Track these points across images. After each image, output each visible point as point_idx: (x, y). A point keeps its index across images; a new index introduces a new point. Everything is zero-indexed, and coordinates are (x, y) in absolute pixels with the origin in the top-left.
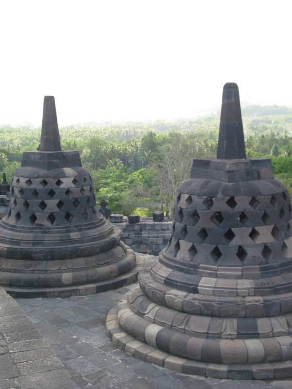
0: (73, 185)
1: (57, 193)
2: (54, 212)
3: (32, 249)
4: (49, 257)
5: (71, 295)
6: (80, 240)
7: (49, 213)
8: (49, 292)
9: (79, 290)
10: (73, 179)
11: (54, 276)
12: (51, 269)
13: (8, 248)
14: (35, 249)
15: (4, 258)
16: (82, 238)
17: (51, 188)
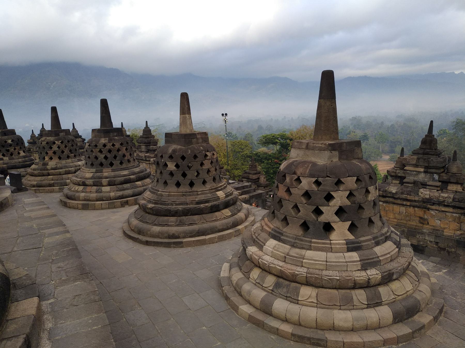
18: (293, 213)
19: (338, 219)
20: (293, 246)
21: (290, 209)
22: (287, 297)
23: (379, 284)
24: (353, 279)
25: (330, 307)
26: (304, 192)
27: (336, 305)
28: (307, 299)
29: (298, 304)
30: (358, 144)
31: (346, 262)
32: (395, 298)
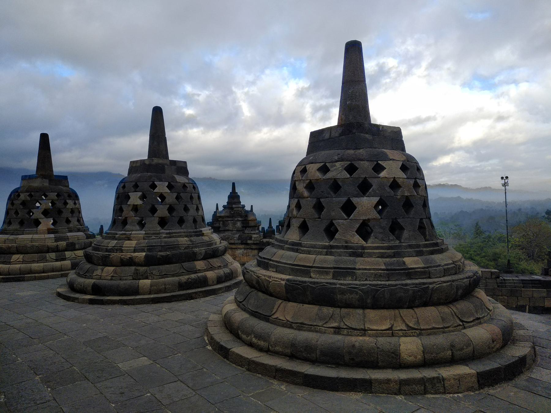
0: (402, 175)
2: (369, 220)
5: (426, 392)
6: (424, 273)
7: (361, 221)
8: (376, 380)
9: (444, 379)
10: (400, 164)
11: (384, 342)
12: (375, 327)
13: (288, 280)
14: (341, 284)
15: (279, 298)
16: (428, 268)
19: (44, 217)
20: (12, 235)
22: (3, 262)
25: (31, 262)
26: (21, 201)
28: (17, 260)
29: (10, 264)
30: (65, 178)
31: (45, 238)
32: (76, 257)
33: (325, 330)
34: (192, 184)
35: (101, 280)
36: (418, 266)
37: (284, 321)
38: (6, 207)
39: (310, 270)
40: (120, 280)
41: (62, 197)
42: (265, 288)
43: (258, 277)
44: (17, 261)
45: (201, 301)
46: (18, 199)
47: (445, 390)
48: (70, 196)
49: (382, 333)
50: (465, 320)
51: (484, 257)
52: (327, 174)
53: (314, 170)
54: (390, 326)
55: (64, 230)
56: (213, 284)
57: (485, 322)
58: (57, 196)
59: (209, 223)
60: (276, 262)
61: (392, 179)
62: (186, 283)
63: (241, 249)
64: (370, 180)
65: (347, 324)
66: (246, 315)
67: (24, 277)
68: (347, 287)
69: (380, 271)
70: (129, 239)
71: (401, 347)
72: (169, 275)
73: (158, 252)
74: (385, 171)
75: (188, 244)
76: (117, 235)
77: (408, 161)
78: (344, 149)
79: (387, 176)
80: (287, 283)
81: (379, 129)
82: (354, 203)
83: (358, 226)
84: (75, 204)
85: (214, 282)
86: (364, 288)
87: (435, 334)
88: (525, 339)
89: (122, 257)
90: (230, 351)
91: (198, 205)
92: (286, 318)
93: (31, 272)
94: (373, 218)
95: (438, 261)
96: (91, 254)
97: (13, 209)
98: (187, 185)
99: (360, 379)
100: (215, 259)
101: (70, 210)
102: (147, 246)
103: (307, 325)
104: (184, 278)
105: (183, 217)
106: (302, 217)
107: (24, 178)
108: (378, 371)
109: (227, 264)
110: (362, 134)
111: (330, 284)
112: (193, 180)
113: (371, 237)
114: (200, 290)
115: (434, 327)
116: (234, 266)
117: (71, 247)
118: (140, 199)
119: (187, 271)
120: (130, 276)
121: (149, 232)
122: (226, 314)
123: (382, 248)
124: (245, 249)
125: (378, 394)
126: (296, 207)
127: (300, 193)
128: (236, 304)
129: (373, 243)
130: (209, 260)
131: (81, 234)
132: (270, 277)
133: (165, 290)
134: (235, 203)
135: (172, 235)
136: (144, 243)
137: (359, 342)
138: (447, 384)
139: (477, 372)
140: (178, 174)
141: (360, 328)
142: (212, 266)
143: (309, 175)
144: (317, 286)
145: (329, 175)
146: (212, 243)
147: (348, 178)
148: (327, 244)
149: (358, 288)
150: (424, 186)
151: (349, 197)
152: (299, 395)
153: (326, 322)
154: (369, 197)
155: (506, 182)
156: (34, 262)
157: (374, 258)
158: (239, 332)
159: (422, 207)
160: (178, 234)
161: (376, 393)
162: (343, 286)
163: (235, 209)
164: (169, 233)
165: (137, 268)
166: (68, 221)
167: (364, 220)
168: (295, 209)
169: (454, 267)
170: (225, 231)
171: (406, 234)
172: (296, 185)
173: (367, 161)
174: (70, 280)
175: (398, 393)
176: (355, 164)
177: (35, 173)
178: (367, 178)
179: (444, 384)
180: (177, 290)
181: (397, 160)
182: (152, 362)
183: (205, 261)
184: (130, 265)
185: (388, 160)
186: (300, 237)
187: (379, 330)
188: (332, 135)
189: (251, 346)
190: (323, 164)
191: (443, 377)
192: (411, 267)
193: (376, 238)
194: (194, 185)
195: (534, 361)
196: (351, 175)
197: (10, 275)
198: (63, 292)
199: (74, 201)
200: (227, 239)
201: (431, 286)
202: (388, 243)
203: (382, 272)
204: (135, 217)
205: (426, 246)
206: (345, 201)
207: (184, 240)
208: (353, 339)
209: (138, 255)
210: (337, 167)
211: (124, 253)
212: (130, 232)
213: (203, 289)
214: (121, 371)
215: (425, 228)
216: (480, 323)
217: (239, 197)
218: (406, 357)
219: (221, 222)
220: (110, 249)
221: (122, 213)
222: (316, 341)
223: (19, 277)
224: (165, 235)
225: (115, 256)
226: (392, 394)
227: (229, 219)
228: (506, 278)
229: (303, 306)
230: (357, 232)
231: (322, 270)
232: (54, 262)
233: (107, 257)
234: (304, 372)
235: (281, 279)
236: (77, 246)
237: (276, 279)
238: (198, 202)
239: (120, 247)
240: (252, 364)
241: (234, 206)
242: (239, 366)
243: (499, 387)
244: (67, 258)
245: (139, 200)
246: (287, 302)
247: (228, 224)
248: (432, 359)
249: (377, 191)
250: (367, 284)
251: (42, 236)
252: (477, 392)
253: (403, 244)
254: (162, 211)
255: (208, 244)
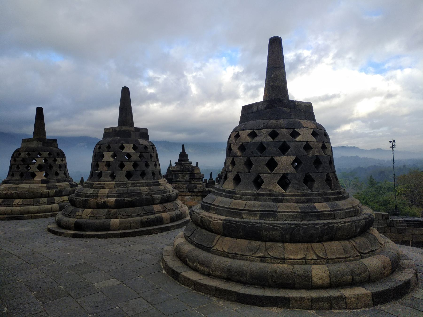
0: (313, 139)
1: (292, 148)
2: (287, 174)
3: (261, 223)
4: (288, 236)
5: (331, 308)
7: (282, 175)
8: (293, 298)
9: (346, 298)
10: (312, 131)
11: (299, 268)
12: (292, 257)
13: (225, 220)
14: (266, 223)
15: (218, 234)
16: (333, 211)
17: (283, 140)
18: (16, 170)
20: (14, 184)
21: (15, 168)
22: (7, 205)
23: (55, 196)
24: (40, 192)
26: (21, 159)
27: (32, 204)
28: (17, 203)
29: (12, 207)
30: (55, 141)
31: (39, 187)
33: (253, 259)
34: (151, 145)
35: (81, 219)
36: (325, 210)
37: (222, 251)
38: (10, 162)
39: (242, 212)
40: (96, 219)
41: (52, 156)
42: (207, 225)
43: (202, 217)
44: (18, 204)
45: (158, 236)
46: (19, 157)
47: (347, 306)
48: (58, 155)
49: (297, 262)
50: (362, 252)
51: (377, 202)
52: (255, 138)
53: (245, 135)
54: (304, 256)
55: (54, 181)
56: (167, 223)
57: (378, 254)
58: (48, 154)
59: (165, 176)
60: (216, 206)
61: (305, 143)
62: (146, 222)
63: (189, 195)
64: (288, 143)
65: (271, 255)
66: (192, 247)
67: (23, 217)
68: (271, 226)
69: (296, 214)
70: (103, 188)
71: (312, 273)
72: (133, 216)
73: (126, 198)
74: (300, 136)
75: (148, 192)
76: (94, 184)
77: (317, 129)
78: (268, 119)
79: (301, 140)
80: (224, 222)
81: (295, 104)
82: (276, 161)
83: (279, 179)
84: (62, 160)
85: (167, 221)
86: (283, 226)
87: (338, 262)
88: (409, 267)
89: (98, 201)
90: (180, 275)
91: (156, 162)
92: (223, 249)
93: (28, 212)
94: (290, 172)
95: (341, 206)
96: (74, 199)
97: (15, 164)
98: (148, 147)
99: (280, 297)
100: (169, 203)
101: (58, 165)
102: (117, 193)
103: (239, 255)
104: (145, 218)
105: (145, 171)
106: (236, 172)
107: (24, 141)
108: (295, 291)
109: (178, 207)
110: (282, 108)
111: (258, 223)
112: (152, 143)
113: (289, 187)
114: (157, 227)
115: (338, 257)
116: (183, 209)
117: (59, 193)
118: (112, 157)
119: (147, 212)
120: (104, 216)
121: (119, 182)
122: (177, 246)
123: (298, 195)
124: (191, 195)
125: (294, 309)
126: (231, 163)
127: (235, 153)
128: (184, 238)
129: (290, 191)
130: (164, 204)
131: (67, 183)
132: (211, 217)
133: (130, 226)
134: (184, 161)
135: (136, 185)
136: (115, 191)
137: (280, 269)
138: (348, 301)
139: (372, 293)
140: (140, 138)
141: (281, 257)
142: (166, 208)
143: (241, 139)
144: (248, 225)
145: (257, 139)
146: (167, 191)
147: (272, 142)
148: (255, 192)
149: (279, 226)
150: (330, 148)
151: (272, 156)
152: (233, 309)
153: (255, 253)
154: (287, 156)
155: (393, 145)
156: (30, 205)
157: (292, 203)
158: (187, 260)
159: (328, 164)
160: (141, 184)
161: (293, 308)
162: (267, 225)
163: (184, 165)
164: (134, 183)
165: (109, 210)
166: (57, 174)
167: (284, 174)
168: (230, 164)
169: (354, 211)
170: (176, 181)
171: (316, 185)
172: (231, 146)
173: (286, 128)
174: (58, 219)
175: (311, 308)
176: (276, 131)
177: (32, 137)
178: (286, 142)
179: (346, 302)
180: (140, 227)
181: (309, 128)
182: (120, 283)
183: (161, 205)
184: (104, 208)
185: (302, 128)
186: (234, 187)
187: (296, 259)
188: (259, 109)
189: (197, 271)
190: (252, 130)
191: (345, 296)
192: (320, 210)
193: (293, 188)
194: (153, 146)
195: (417, 284)
196: (273, 139)
197: (12, 214)
198: (52, 228)
199: (61, 158)
200: (178, 188)
201: (336, 225)
202: (302, 192)
203: (298, 214)
204: (108, 171)
205: (332, 194)
206: (269, 159)
207: (145, 189)
208: (275, 266)
209: (110, 200)
210: (263, 133)
211: (99, 198)
212: (104, 183)
213: (160, 227)
214: (96, 289)
215: (331, 180)
216: (374, 254)
217: (187, 156)
218: (316, 280)
219: (174, 175)
220: (89, 195)
221: (98, 168)
222: (246, 267)
223: (19, 217)
224: (131, 185)
225: (92, 200)
226: (305, 309)
227: (180, 173)
228: (393, 219)
229: (236, 240)
230: (278, 183)
231: (252, 213)
232: (46, 205)
233: (86, 201)
234: (237, 291)
235: (220, 219)
236: (63, 193)
237: (215, 219)
238: (156, 160)
239: (96, 193)
240: (197, 285)
241: (183, 162)
242: (187, 286)
243: (389, 304)
244: (56, 202)
245: (111, 158)
246: (224, 237)
247: (179, 176)
248: (336, 282)
249: (294, 152)
250: (286, 224)
251: (37, 185)
252: (372, 308)
253: (314, 193)
254: (129, 166)
255: (163, 192)
